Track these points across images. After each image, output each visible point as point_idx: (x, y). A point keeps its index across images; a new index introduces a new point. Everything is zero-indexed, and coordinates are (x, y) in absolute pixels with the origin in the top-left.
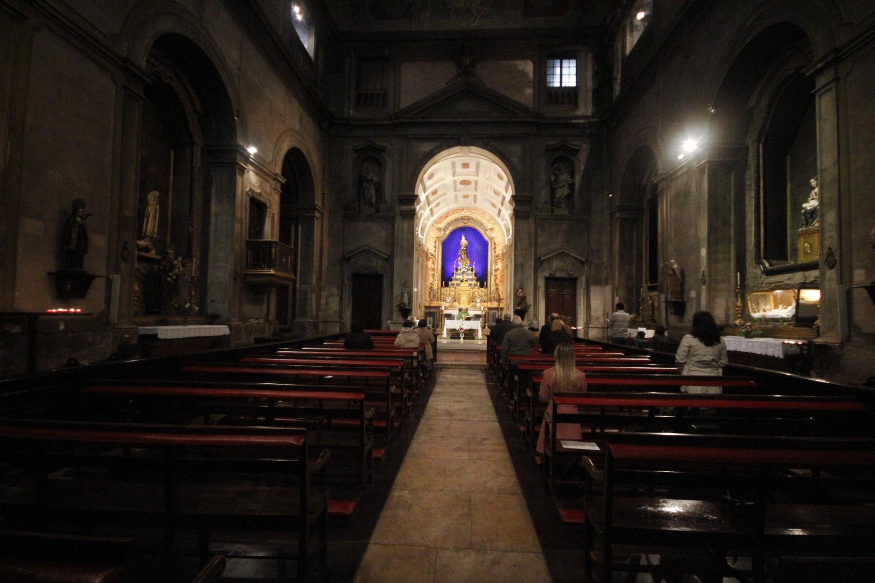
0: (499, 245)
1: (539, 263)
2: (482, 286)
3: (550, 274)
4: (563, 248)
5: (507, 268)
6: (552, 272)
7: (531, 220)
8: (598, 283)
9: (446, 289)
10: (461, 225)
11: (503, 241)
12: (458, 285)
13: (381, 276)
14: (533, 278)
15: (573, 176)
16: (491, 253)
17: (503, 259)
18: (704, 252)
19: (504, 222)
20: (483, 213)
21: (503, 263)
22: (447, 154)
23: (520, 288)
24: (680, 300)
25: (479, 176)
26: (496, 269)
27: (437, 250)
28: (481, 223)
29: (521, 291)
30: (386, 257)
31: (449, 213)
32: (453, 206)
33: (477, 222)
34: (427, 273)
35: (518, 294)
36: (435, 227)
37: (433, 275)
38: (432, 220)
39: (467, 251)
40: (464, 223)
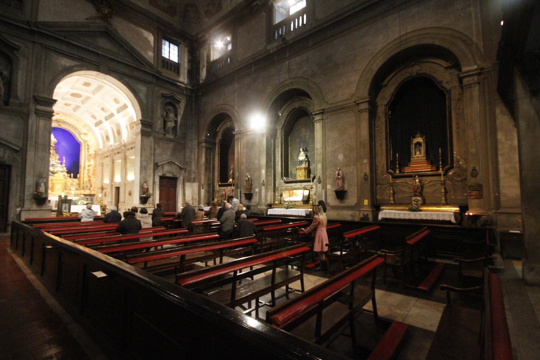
1: (156, 166)
2: (75, 177)
3: (163, 174)
4: (172, 159)
6: (164, 173)
7: (151, 139)
8: (189, 181)
13: (9, 167)
14: (152, 176)
15: (176, 116)
18: (263, 171)
21: (95, 161)
24: (250, 193)
26: (89, 164)
29: (146, 185)
35: (144, 186)
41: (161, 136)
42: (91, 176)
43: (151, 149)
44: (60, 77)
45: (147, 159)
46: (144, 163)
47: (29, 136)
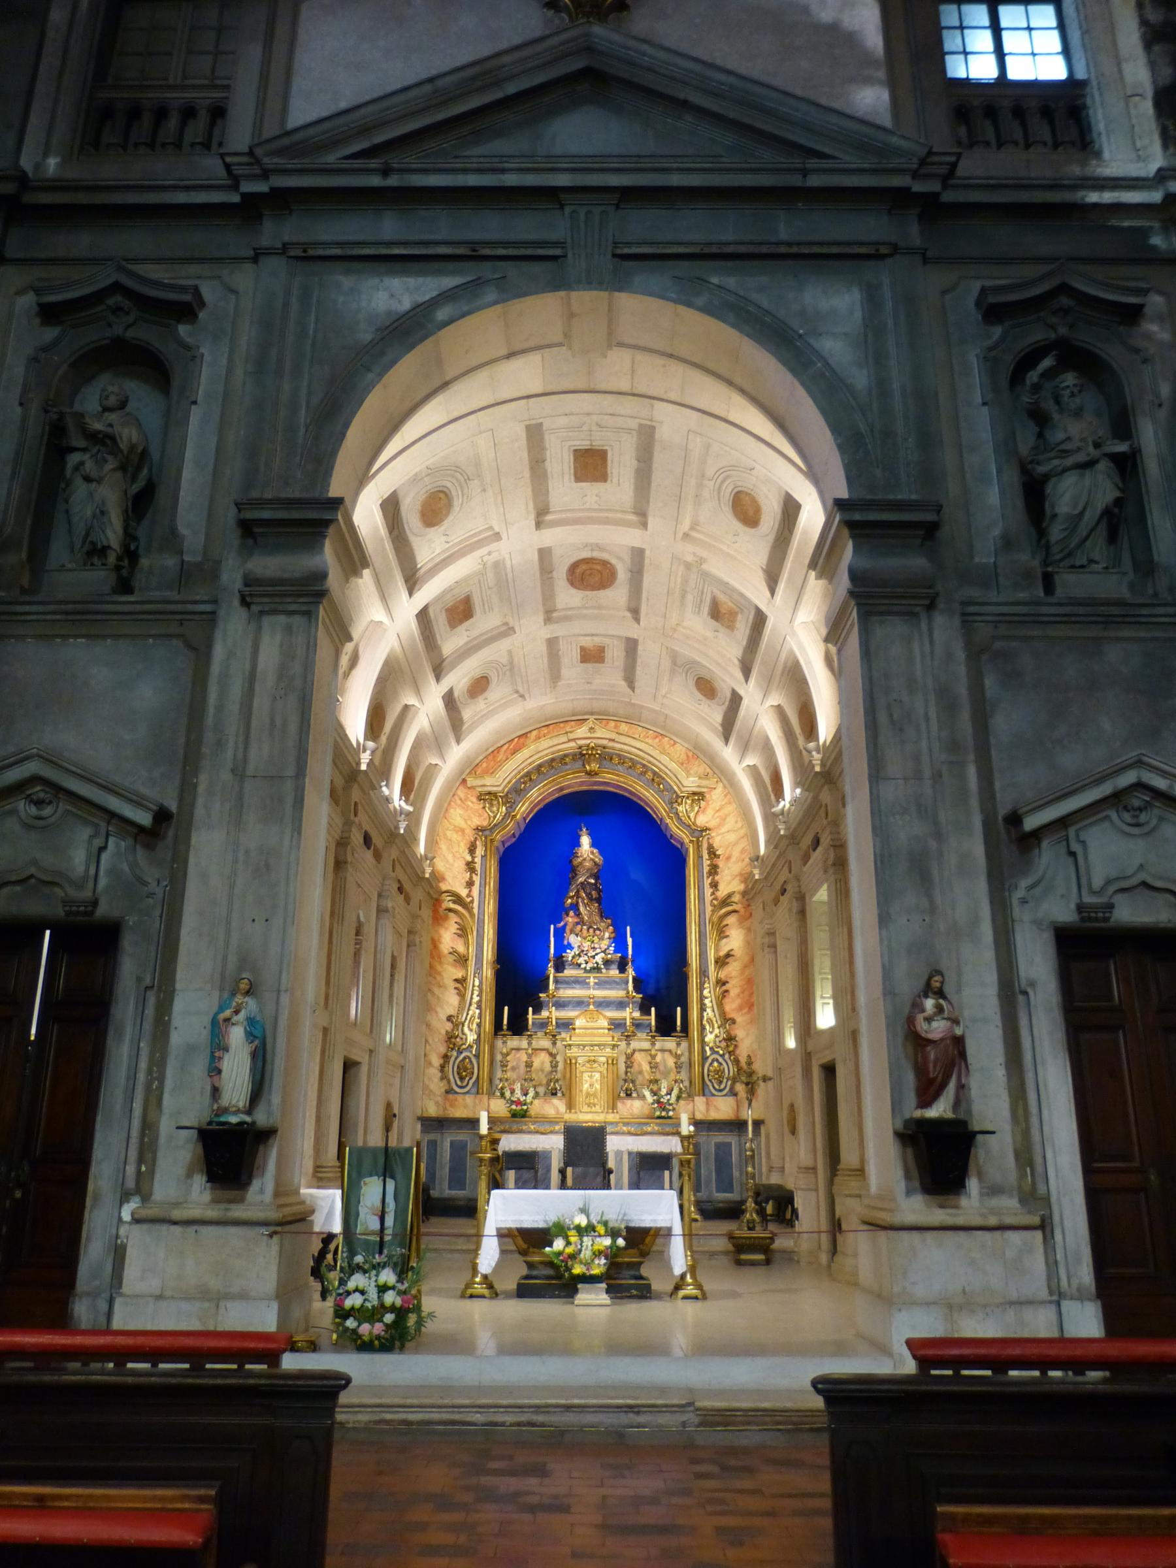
0: (728, 858)
2: (665, 1027)
3: (1080, 908)
4: (1139, 763)
5: (773, 946)
6: (1088, 899)
9: (514, 1042)
10: (573, 781)
11: (744, 844)
12: (567, 1025)
16: (701, 889)
17: (751, 915)
19: (752, 760)
20: (664, 730)
21: (749, 930)
22: (504, 352)
23: (928, 990)
25: (651, 522)
26: (722, 954)
27: (477, 879)
28: (655, 773)
29: (940, 1009)
30: (144, 818)
32: (542, 702)
34: (432, 971)
35: (921, 1026)
36: (472, 788)
37: (462, 981)
38: (457, 754)
39: (599, 891)
41: (1022, 595)
42: (732, 1015)
43: (949, 706)
44: (370, 376)
45: (928, 790)
46: (908, 830)
47: (209, 737)
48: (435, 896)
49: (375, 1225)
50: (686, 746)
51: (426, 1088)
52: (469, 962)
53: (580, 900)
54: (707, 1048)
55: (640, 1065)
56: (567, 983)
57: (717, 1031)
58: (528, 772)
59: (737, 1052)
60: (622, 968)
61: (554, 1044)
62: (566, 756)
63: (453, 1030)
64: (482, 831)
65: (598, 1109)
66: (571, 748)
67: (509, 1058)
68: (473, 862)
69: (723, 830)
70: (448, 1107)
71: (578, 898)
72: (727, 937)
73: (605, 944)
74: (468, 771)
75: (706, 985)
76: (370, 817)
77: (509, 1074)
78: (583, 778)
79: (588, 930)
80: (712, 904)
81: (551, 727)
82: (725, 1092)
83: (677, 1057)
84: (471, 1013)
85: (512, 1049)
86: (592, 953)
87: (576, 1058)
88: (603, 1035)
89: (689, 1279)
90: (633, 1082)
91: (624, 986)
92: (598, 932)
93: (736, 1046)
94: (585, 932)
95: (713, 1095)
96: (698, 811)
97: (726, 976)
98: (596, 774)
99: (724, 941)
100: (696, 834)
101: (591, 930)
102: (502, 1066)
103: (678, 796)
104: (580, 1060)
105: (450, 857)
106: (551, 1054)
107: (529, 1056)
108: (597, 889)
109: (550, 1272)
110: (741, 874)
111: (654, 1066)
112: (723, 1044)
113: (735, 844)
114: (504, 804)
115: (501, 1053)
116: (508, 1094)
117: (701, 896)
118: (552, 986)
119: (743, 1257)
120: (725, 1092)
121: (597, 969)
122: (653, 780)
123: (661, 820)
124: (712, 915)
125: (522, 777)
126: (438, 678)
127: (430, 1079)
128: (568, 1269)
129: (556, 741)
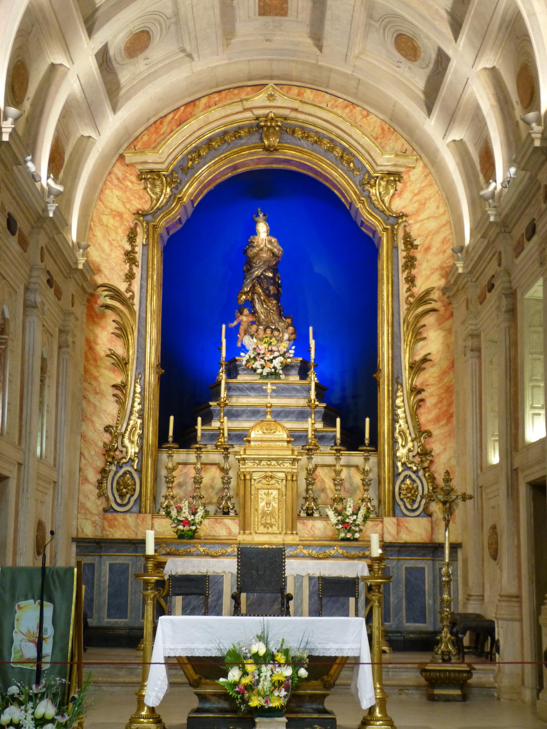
0: (428, 249)
5: (478, 350)
9: (181, 455)
11: (445, 233)
17: (452, 314)
26: (418, 358)
27: (137, 271)
28: (344, 149)
31: (193, 103)
33: (327, 145)
36: (131, 165)
37: (121, 387)
40: (267, 149)
42: (429, 427)
48: (90, 291)
49: (31, 652)
50: (382, 117)
51: (81, 506)
52: (129, 366)
53: (256, 297)
54: (399, 464)
55: (323, 481)
56: (241, 390)
57: (410, 445)
58: (196, 147)
59: (433, 468)
60: (304, 374)
61: (226, 457)
62: (240, 128)
63: (111, 442)
64: (143, 215)
65: (275, 529)
66: (247, 119)
67: (174, 474)
68: (133, 251)
69: (423, 216)
70: (107, 528)
71: (253, 293)
72: (425, 339)
73: (284, 346)
74: (126, 145)
75: (399, 394)
76: (14, 198)
77: (175, 492)
78: (261, 154)
79: (265, 330)
80: (407, 301)
81: (223, 93)
82: (417, 513)
83: (365, 473)
84: (132, 423)
85: (179, 464)
86: (269, 357)
87: (251, 473)
88: (282, 448)
89: (378, 714)
90: (315, 500)
91: (305, 394)
92: (276, 333)
93: (431, 462)
94: (261, 332)
95: (406, 516)
96: (394, 194)
97: (422, 384)
98: (276, 150)
99: (421, 343)
100: (392, 220)
101: (268, 331)
102: (167, 482)
103: (370, 177)
104: (255, 476)
105: (106, 246)
106: (222, 470)
107: (198, 471)
108: (275, 284)
109: (225, 705)
110: (442, 268)
111: (338, 483)
112: (417, 459)
113: (437, 232)
114: (169, 184)
115: (166, 468)
116: (174, 513)
117: (395, 293)
118: (223, 394)
119: (437, 692)
120: (417, 513)
121: (274, 374)
122: (342, 157)
123: (351, 204)
124: (407, 314)
125: (190, 153)
126: (90, 32)
127: (86, 496)
128: (245, 701)
129: (229, 110)
